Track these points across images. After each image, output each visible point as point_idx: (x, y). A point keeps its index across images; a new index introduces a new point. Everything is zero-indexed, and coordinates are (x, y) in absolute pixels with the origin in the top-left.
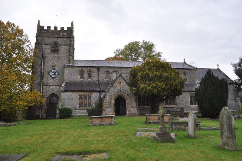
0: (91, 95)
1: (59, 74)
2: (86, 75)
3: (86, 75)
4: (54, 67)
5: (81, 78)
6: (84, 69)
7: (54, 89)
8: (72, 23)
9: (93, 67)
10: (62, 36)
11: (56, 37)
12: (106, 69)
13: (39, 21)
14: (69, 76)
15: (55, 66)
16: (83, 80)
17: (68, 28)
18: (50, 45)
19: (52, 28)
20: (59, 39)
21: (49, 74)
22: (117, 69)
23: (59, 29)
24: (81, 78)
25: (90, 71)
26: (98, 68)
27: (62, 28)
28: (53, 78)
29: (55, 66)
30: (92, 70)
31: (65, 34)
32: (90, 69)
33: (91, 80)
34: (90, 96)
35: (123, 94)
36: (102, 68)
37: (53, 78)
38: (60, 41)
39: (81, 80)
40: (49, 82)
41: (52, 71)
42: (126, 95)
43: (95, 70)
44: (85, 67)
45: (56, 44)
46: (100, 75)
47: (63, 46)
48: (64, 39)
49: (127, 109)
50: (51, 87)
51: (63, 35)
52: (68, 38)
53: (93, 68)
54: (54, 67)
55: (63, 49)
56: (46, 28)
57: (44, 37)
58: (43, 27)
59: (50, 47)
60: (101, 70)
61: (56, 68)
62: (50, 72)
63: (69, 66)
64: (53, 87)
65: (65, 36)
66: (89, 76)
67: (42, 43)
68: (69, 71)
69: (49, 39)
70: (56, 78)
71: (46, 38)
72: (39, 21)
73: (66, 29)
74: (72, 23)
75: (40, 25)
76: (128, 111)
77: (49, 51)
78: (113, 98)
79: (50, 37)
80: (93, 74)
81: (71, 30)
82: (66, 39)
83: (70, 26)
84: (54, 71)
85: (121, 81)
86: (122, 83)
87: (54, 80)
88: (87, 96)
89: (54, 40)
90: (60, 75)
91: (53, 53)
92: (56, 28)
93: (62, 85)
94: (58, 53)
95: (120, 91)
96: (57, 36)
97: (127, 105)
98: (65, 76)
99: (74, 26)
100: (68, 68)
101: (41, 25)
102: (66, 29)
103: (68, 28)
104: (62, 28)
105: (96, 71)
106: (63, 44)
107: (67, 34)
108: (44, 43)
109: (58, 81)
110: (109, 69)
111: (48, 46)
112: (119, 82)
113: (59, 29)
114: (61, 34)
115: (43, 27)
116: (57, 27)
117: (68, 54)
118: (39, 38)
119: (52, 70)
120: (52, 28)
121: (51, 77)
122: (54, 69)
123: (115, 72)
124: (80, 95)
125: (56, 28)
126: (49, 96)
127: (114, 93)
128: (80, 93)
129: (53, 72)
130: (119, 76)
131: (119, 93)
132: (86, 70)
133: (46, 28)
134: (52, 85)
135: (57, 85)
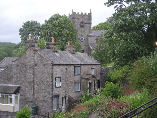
1: (85, 40)
4: (82, 36)
8: (91, 10)
13: (73, 9)
15: (82, 35)
19: (80, 14)
21: (80, 39)
23: (84, 14)
27: (85, 13)
29: (82, 35)
31: (87, 17)
38: (85, 21)
45: (82, 23)
48: (87, 20)
52: (89, 19)
54: (82, 36)
55: (87, 26)
56: (77, 14)
62: (80, 38)
65: (87, 18)
72: (73, 9)
73: (87, 14)
74: (91, 10)
77: (79, 27)
81: (90, 14)
83: (90, 12)
84: (82, 38)
91: (81, 28)
92: (82, 13)
96: (82, 18)
99: (92, 12)
101: (74, 11)
102: (87, 14)
104: (85, 13)
106: (86, 23)
111: (79, 24)
113: (84, 14)
120: (80, 14)
122: (82, 37)
125: (82, 13)
129: (81, 39)
133: (77, 14)
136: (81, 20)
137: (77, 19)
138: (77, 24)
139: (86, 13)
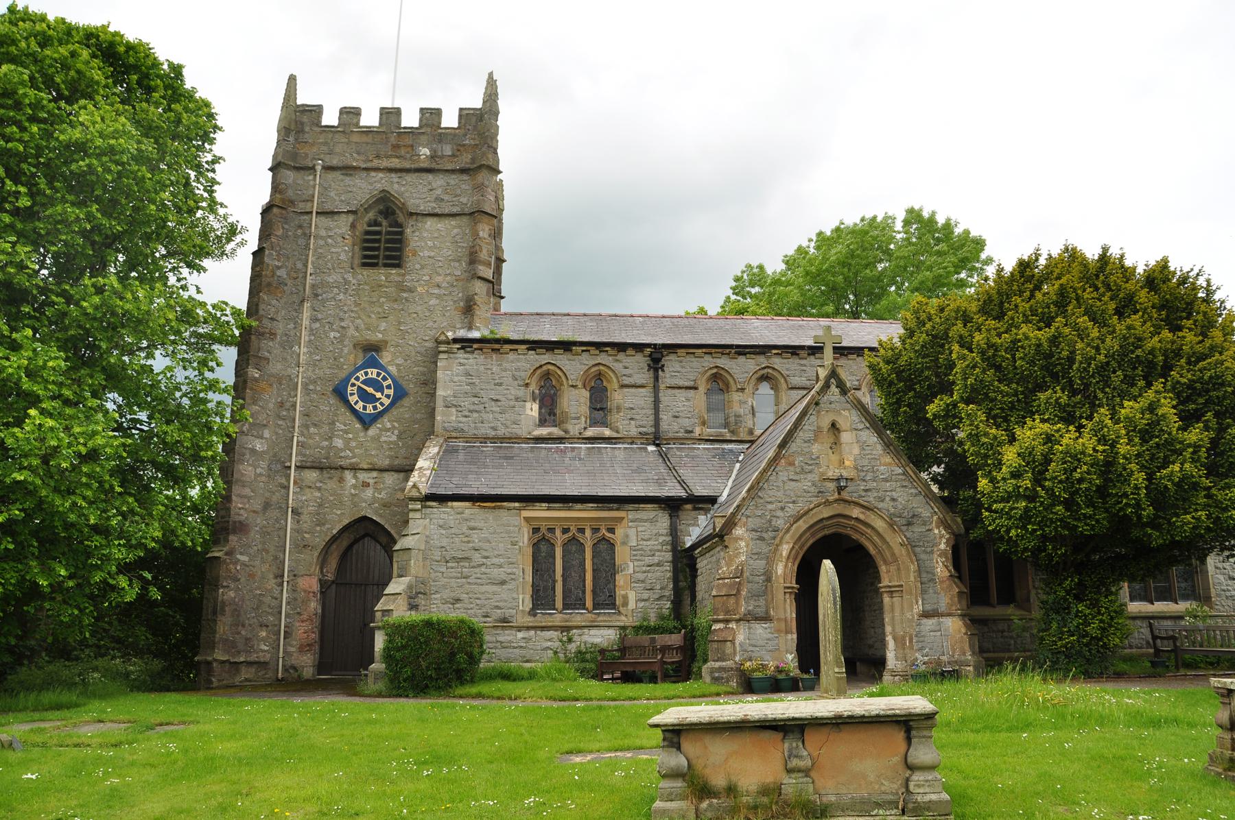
0: (612, 531)
1: (400, 394)
2: (575, 402)
3: (575, 402)
5: (542, 422)
6: (561, 359)
7: (369, 493)
8: (491, 83)
9: (622, 347)
10: (423, 165)
11: (391, 170)
12: (708, 362)
13: (292, 80)
14: (466, 403)
16: (556, 431)
17: (464, 114)
18: (351, 218)
19: (370, 118)
20: (409, 178)
21: (340, 393)
22: (777, 362)
23: (410, 120)
24: (542, 422)
25: (599, 376)
26: (657, 355)
27: (431, 116)
28: (366, 422)
30: (617, 367)
32: (603, 358)
33: (607, 432)
34: (604, 539)
35: (856, 512)
36: (681, 352)
37: (366, 422)
39: (544, 431)
40: (339, 443)
41: (361, 374)
42: (879, 524)
43: (635, 367)
44: (566, 346)
46: (666, 397)
47: (430, 223)
48: (438, 181)
49: (888, 629)
50: (348, 475)
51: (433, 157)
52: (463, 171)
53: (621, 356)
56: (330, 118)
57: (319, 168)
58: (317, 110)
59: (353, 226)
60: (674, 368)
61: (385, 358)
63: (466, 344)
64: (363, 476)
66: (593, 408)
67: (301, 207)
68: (468, 374)
69: (348, 180)
70: (386, 422)
71: (331, 175)
72: (292, 80)
73: (450, 120)
74: (491, 83)
75: (299, 102)
76: (900, 641)
78: (785, 549)
79: (355, 168)
80: (618, 397)
82: (453, 179)
83: (477, 103)
84: (373, 373)
85: (842, 423)
86: (846, 437)
87: (372, 431)
88: (588, 533)
89: (379, 186)
90: (406, 402)
92: (390, 115)
93: (421, 463)
94: (398, 266)
95: (840, 489)
96: (395, 163)
97: (886, 599)
98: (440, 408)
99: (502, 104)
100: (461, 354)
101: (302, 99)
102: (450, 120)
103: (464, 114)
104: (431, 116)
105: (644, 377)
106: (423, 208)
107: (459, 148)
108: (320, 204)
109: (394, 438)
110: (724, 362)
111: (342, 225)
112: (825, 423)
113: (410, 120)
114: (425, 151)
115: (317, 110)
116: (397, 112)
117: (459, 269)
118: (289, 176)
119: (358, 370)
120: (370, 118)
121: (354, 412)
122: (373, 363)
123: (764, 378)
124: (536, 530)
125: (390, 115)
126: (334, 539)
127: (792, 509)
128: (540, 512)
130: (827, 386)
131: (827, 512)
132: (574, 367)
133: (330, 118)
134: (354, 469)
135: (386, 463)
136: (381, 182)
137: (328, 168)
138: (324, 221)
139: (437, 113)
